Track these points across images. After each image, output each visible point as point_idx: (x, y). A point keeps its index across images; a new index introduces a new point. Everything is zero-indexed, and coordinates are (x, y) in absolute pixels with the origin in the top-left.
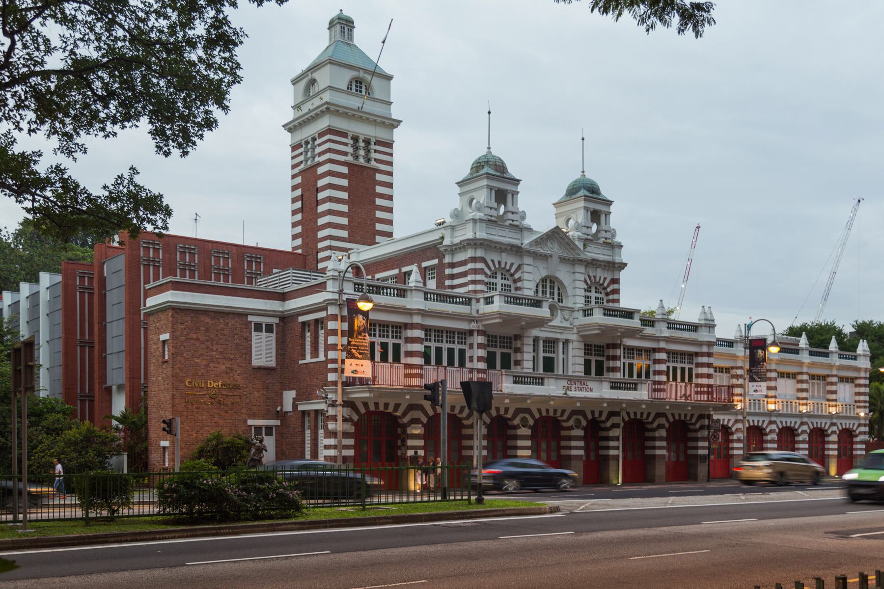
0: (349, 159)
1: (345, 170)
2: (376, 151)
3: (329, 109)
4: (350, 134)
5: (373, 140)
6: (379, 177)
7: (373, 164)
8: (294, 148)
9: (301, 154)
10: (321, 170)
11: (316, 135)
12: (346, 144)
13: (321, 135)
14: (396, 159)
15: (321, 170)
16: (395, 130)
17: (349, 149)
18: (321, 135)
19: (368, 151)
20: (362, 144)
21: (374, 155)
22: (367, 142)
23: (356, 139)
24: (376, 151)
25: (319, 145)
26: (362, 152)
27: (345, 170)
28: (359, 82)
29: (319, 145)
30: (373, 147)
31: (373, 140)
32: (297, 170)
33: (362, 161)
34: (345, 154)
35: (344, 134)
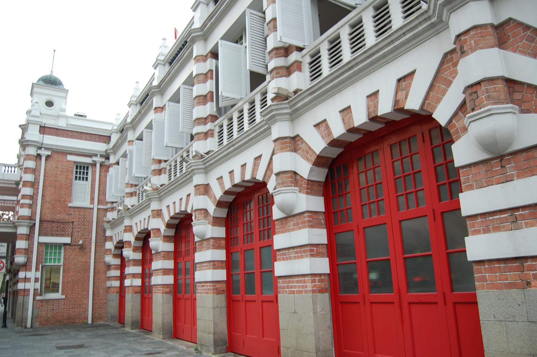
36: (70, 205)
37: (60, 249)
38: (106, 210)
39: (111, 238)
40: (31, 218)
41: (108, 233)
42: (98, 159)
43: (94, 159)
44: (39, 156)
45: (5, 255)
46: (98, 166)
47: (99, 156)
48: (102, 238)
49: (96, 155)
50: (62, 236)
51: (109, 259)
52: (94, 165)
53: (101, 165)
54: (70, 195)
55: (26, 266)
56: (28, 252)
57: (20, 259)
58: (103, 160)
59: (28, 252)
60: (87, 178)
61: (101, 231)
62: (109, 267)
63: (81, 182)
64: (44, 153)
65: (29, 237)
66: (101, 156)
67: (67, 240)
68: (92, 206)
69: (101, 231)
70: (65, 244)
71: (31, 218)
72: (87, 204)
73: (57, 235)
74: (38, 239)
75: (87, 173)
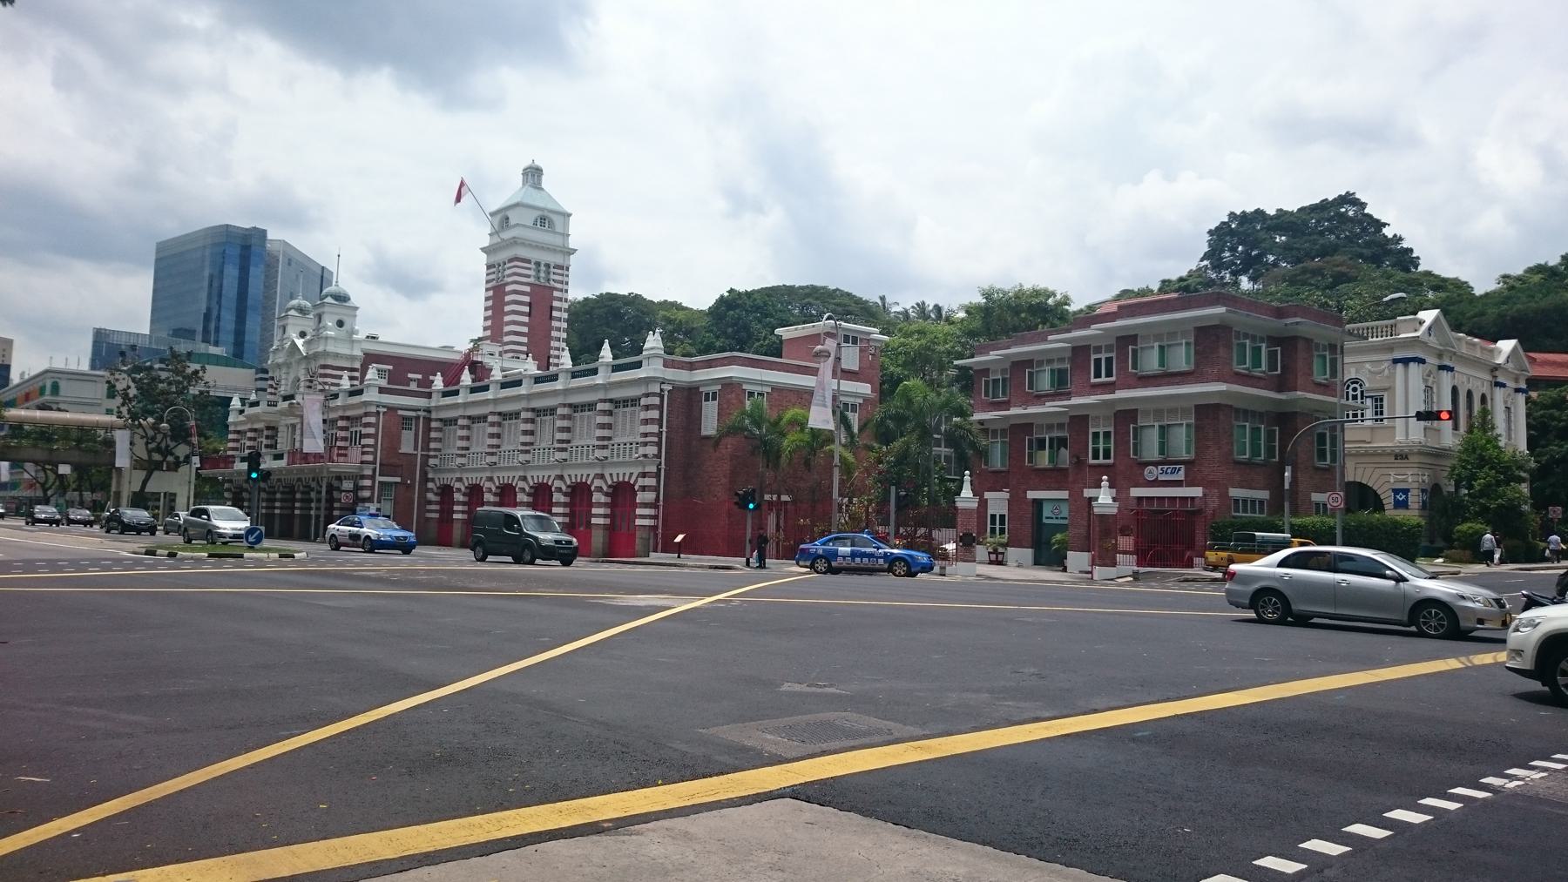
0: (531, 280)
1: (528, 289)
3: (514, 242)
6: (556, 294)
8: (489, 267)
10: (508, 288)
13: (510, 261)
14: (571, 280)
15: (508, 288)
17: (532, 273)
18: (510, 261)
20: (543, 268)
22: (548, 266)
23: (538, 264)
26: (542, 275)
27: (528, 289)
28: (543, 219)
35: (529, 261)
39: (433, 480)
40: (374, 462)
48: (425, 479)
51: (430, 496)
52: (417, 418)
54: (399, 442)
55: (370, 500)
56: (372, 488)
57: (366, 494)
59: (372, 488)
61: (424, 474)
62: (430, 503)
64: (382, 410)
65: (373, 477)
67: (398, 480)
69: (424, 474)
71: (374, 462)
74: (379, 479)
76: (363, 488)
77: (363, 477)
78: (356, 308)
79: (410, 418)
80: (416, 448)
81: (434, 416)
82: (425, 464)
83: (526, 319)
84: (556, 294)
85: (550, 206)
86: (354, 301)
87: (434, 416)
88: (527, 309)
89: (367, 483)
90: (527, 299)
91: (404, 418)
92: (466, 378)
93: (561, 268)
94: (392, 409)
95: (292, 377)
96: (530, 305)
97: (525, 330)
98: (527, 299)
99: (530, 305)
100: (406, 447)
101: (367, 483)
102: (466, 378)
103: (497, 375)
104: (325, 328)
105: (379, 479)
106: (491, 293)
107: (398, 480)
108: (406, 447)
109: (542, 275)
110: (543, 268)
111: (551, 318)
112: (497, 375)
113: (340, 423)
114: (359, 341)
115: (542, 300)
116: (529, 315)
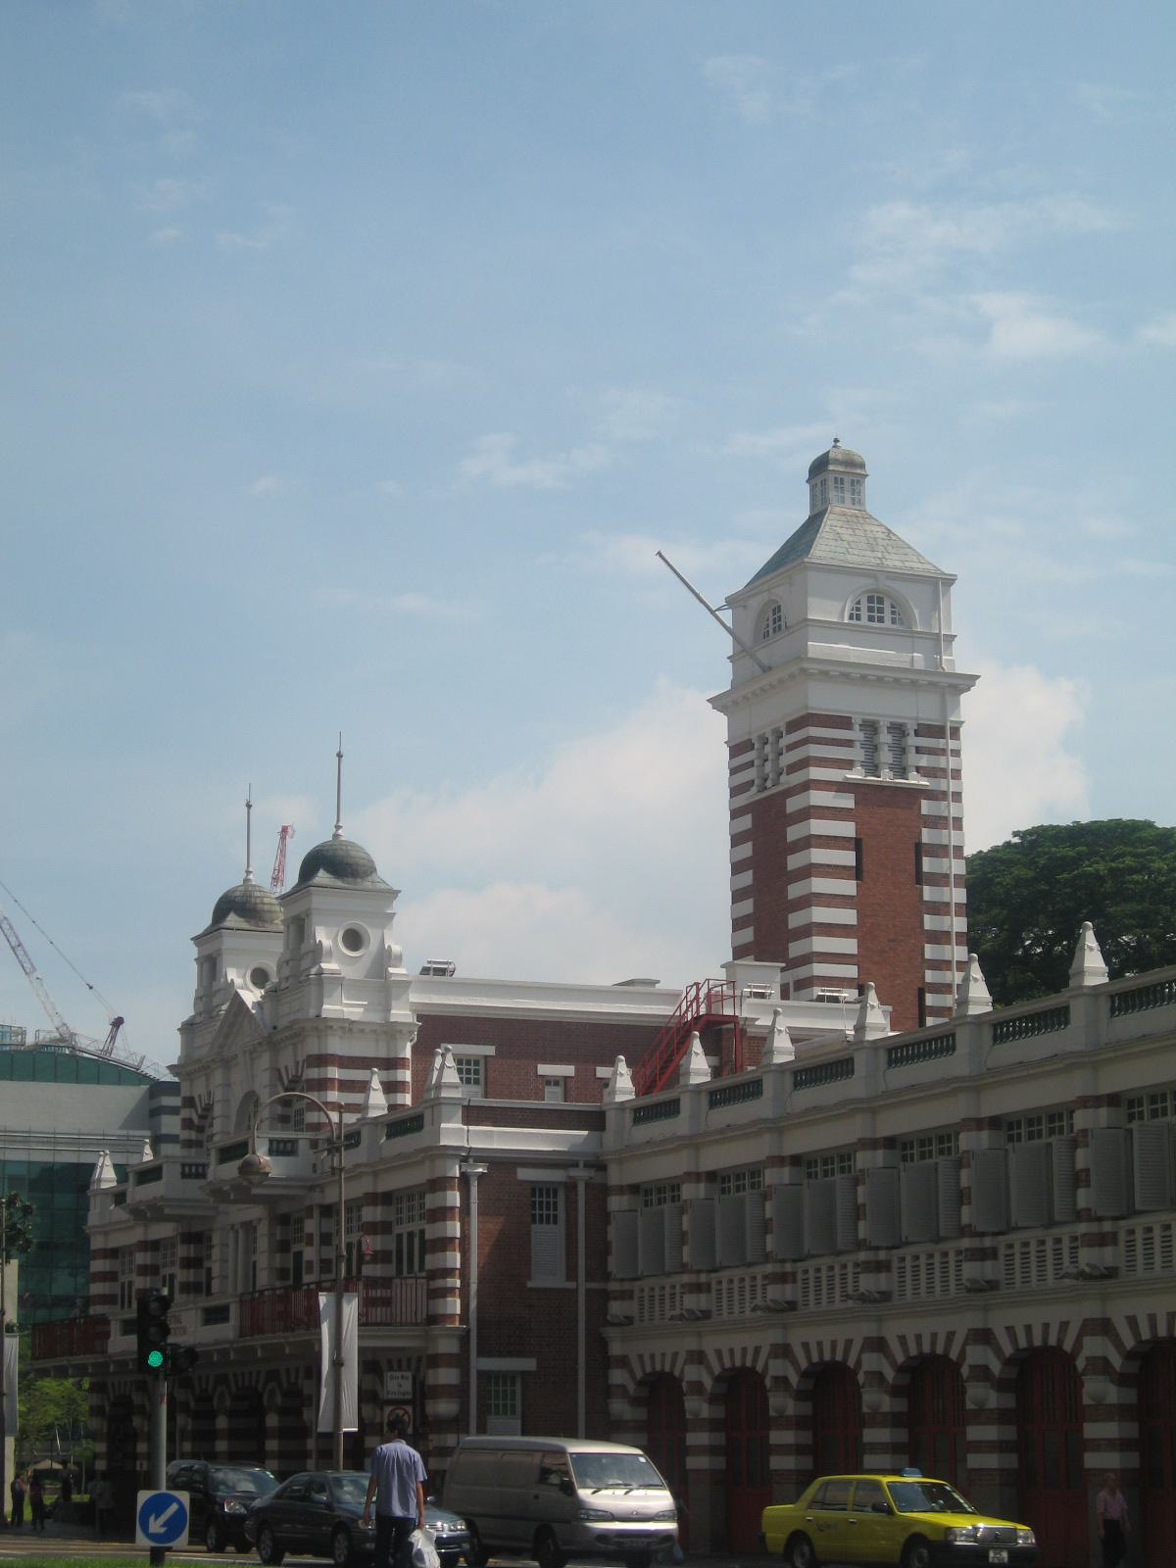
0: (856, 775)
1: (847, 802)
2: (919, 750)
4: (857, 720)
5: (911, 727)
6: (926, 807)
7: (915, 780)
8: (736, 750)
9: (751, 764)
11: (783, 729)
12: (849, 743)
16: (963, 697)
18: (794, 725)
19: (901, 751)
20: (885, 738)
21: (913, 759)
22: (898, 730)
23: (871, 727)
24: (919, 750)
25: (791, 747)
26: (886, 756)
27: (847, 802)
29: (791, 747)
30: (913, 741)
31: (911, 727)
32: (743, 800)
33: (886, 777)
34: (848, 764)
35: (844, 723)
36: (530, 1284)
37: (513, 1384)
38: (606, 1296)
39: (623, 1362)
41: (616, 1349)
42: (581, 1174)
43: (573, 1172)
44: (465, 1179)
45: (410, 1397)
46: (581, 1188)
47: (581, 1164)
48: (602, 1360)
49: (575, 1165)
50: (520, 1354)
52: (571, 1187)
53: (588, 1185)
57: (444, 1407)
58: (592, 1173)
59: (460, 1392)
60: (555, 1216)
63: (544, 1227)
65: (461, 1361)
66: (587, 1165)
67: (529, 1364)
68: (571, 1285)
70: (524, 1374)
72: (557, 1280)
73: (510, 1354)
75: (555, 1203)
76: (438, 1392)
77: (435, 1361)
78: (393, 894)
79: (550, 1189)
80: (571, 1273)
81: (615, 1177)
82: (598, 1315)
83: (848, 887)
84: (926, 807)
85: (893, 562)
86: (386, 871)
87: (615, 1177)
88: (848, 858)
89: (447, 1376)
90: (848, 829)
91: (536, 1188)
92: (699, 1065)
93: (937, 731)
94: (502, 1164)
95: (238, 1094)
96: (857, 844)
97: (848, 916)
98: (848, 829)
99: (857, 844)
100: (547, 1274)
101: (447, 1376)
102: (699, 1065)
103: (783, 1050)
104: (317, 953)
105: (479, 1363)
106: (746, 822)
107: (529, 1364)
108: (547, 1274)
109: (886, 756)
110: (885, 738)
111: (920, 878)
112: (783, 1050)
113: (370, 1214)
114: (404, 985)
115: (897, 822)
116: (858, 873)
